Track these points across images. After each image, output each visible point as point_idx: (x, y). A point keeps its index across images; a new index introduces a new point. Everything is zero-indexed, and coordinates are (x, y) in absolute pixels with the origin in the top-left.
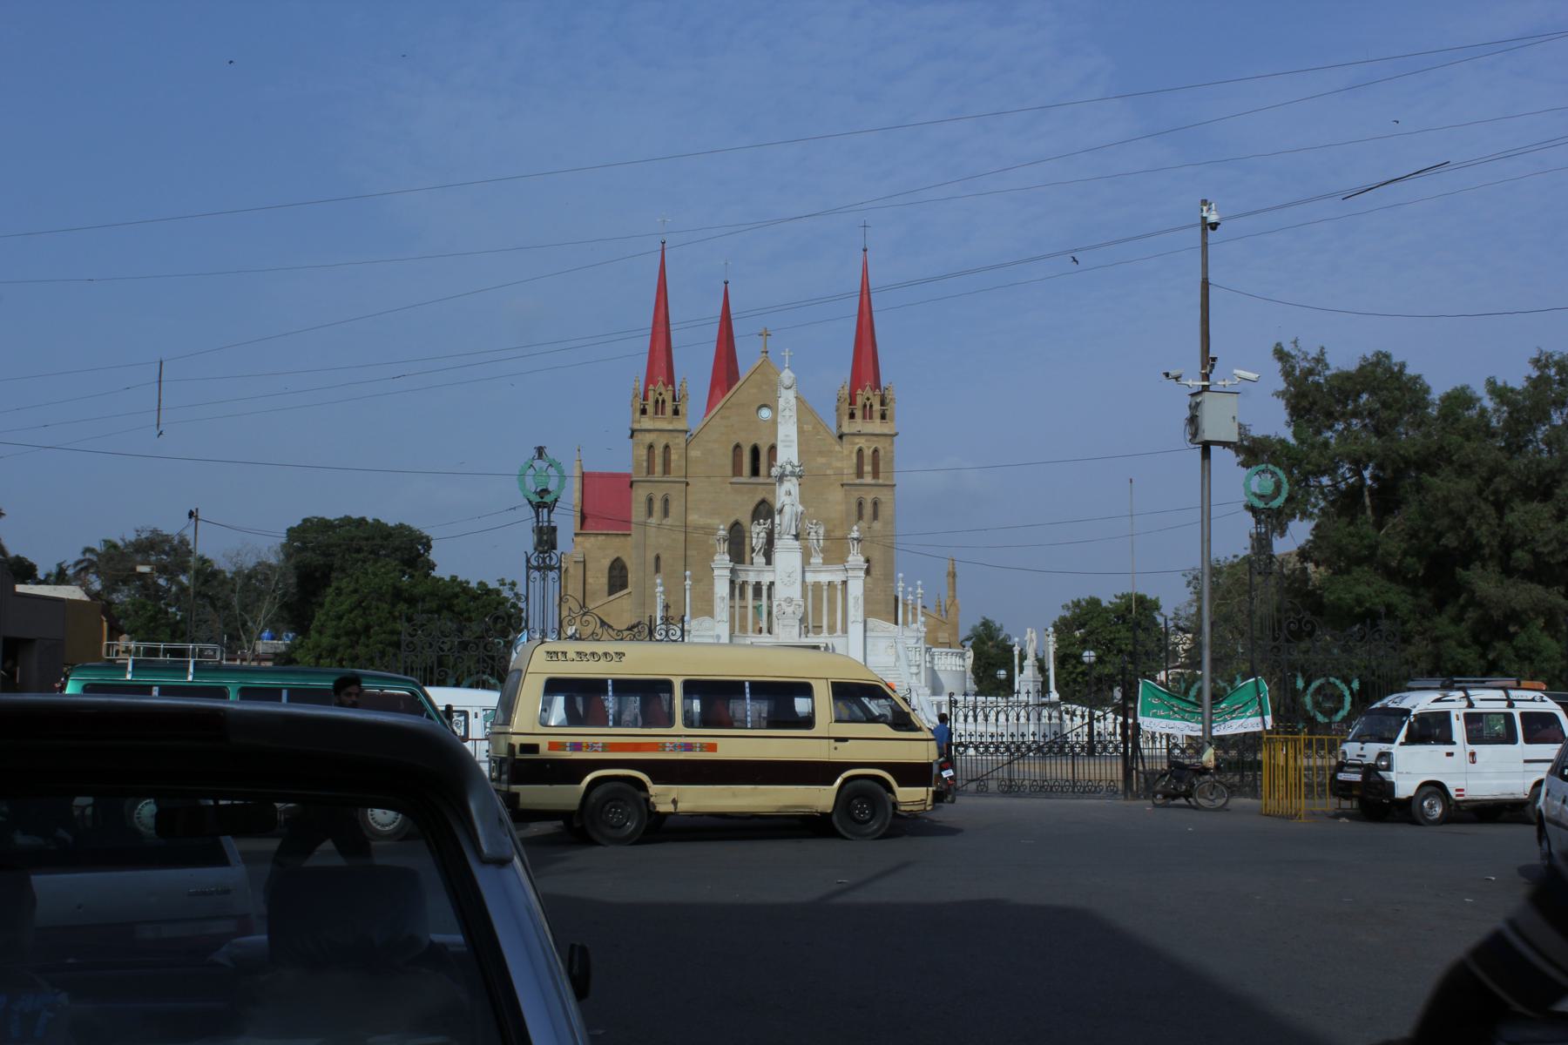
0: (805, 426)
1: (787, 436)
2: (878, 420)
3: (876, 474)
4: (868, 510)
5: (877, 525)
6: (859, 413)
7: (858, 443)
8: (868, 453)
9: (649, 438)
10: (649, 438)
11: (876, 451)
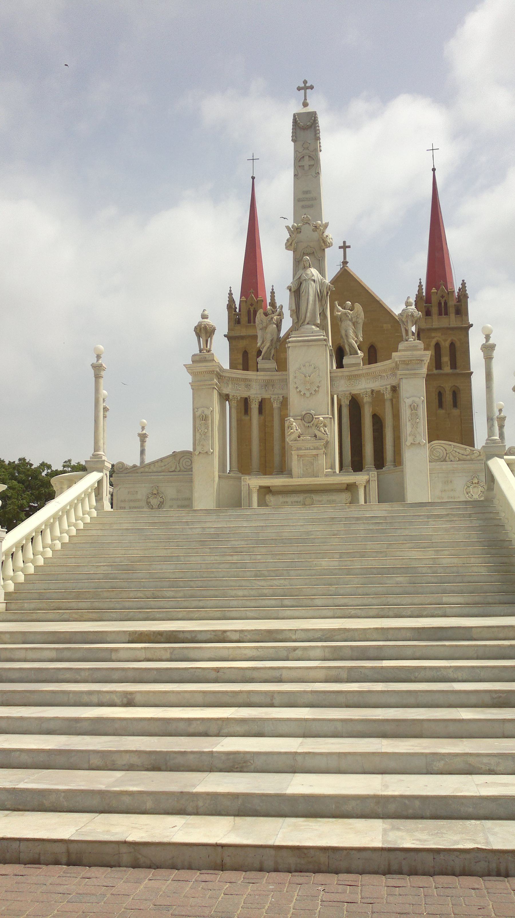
0: (384, 325)
1: (306, 192)
2: (452, 316)
3: (454, 366)
4: (448, 398)
5: (456, 412)
6: (435, 310)
7: (434, 338)
8: (445, 345)
9: (242, 344)
10: (242, 344)
11: (452, 345)
